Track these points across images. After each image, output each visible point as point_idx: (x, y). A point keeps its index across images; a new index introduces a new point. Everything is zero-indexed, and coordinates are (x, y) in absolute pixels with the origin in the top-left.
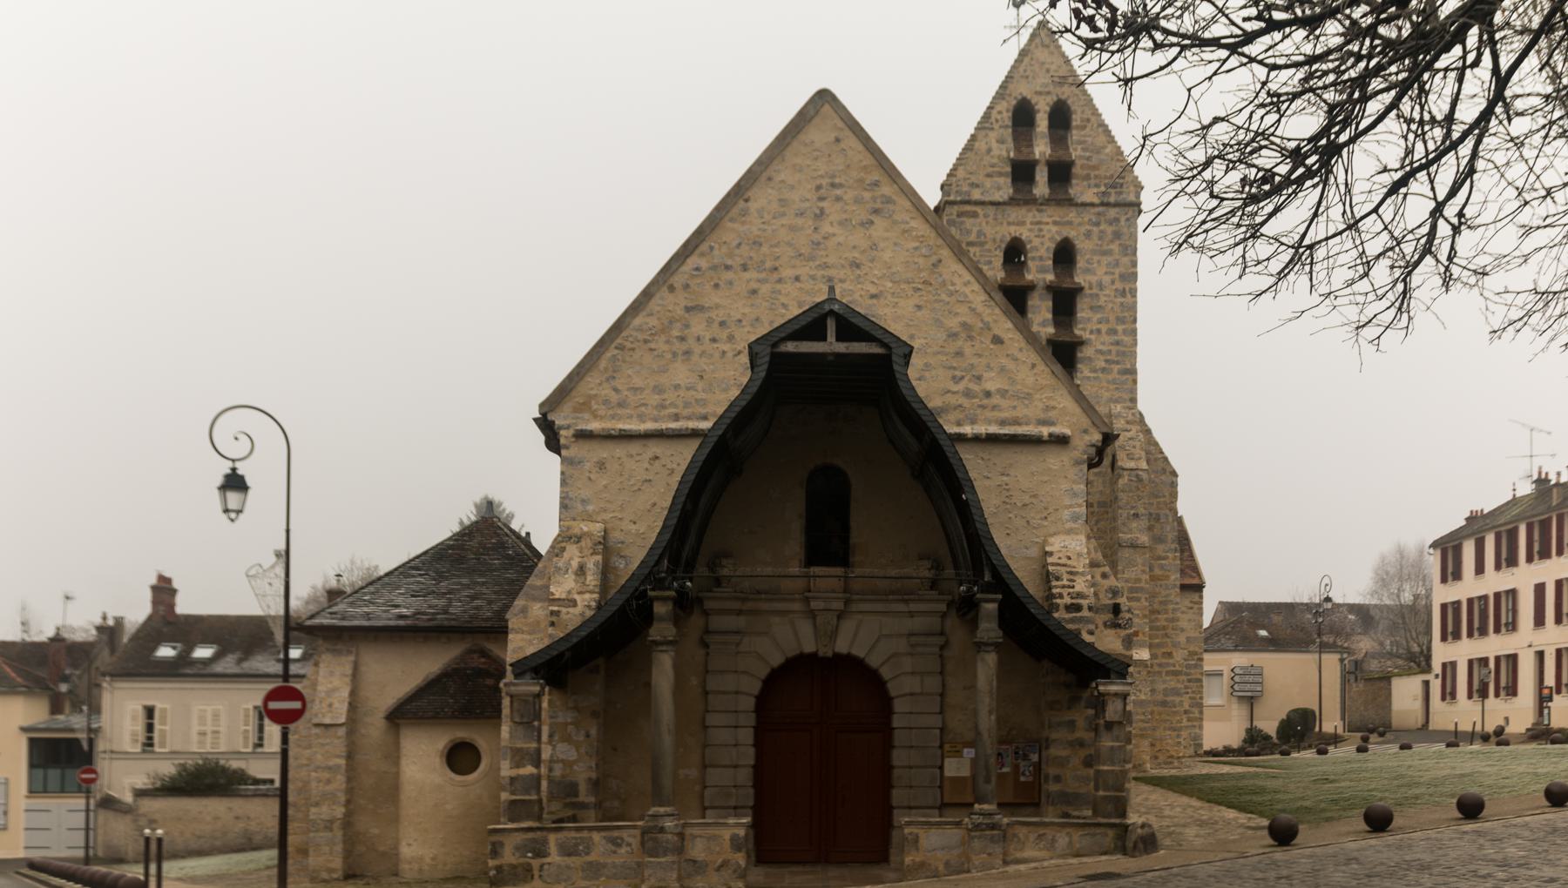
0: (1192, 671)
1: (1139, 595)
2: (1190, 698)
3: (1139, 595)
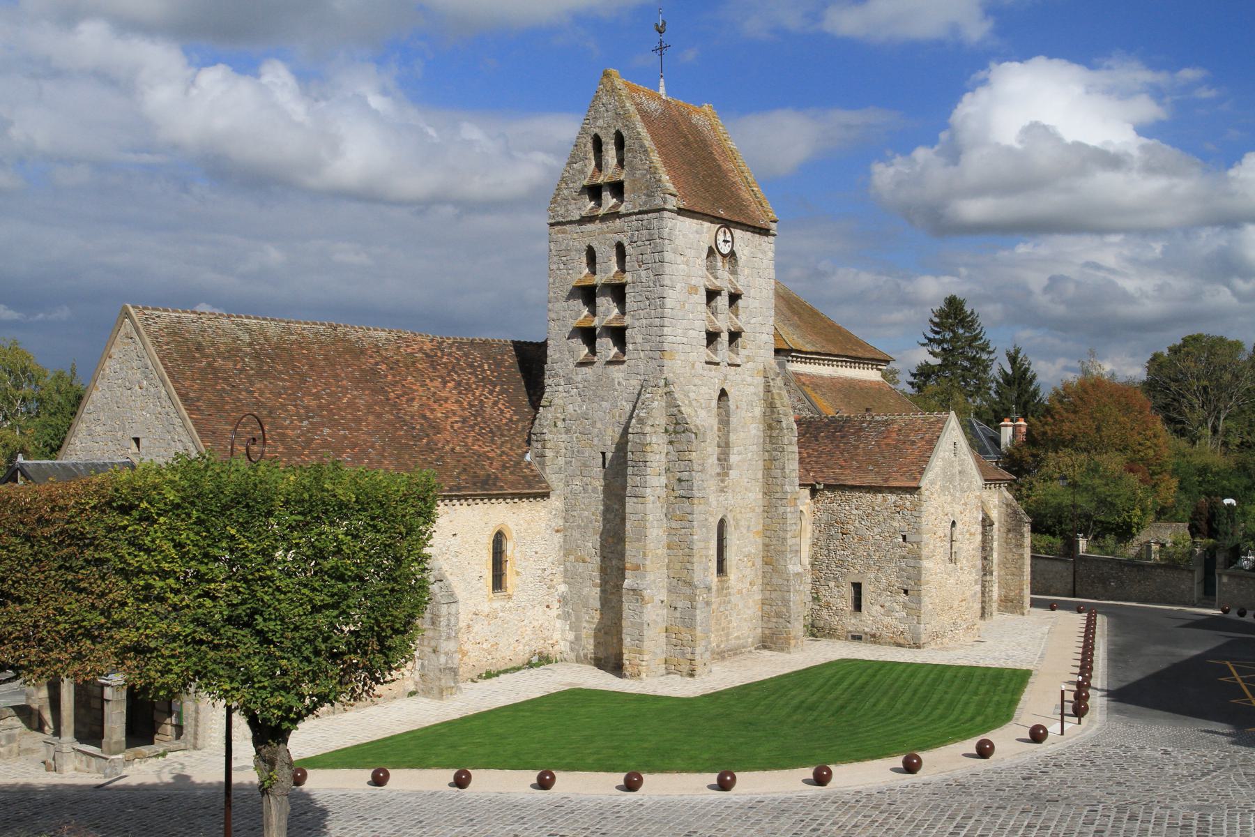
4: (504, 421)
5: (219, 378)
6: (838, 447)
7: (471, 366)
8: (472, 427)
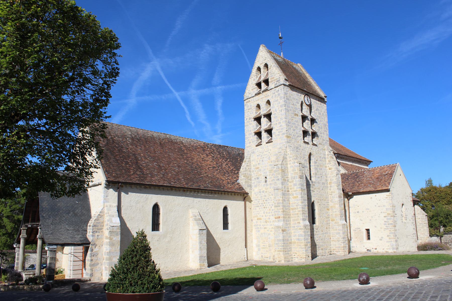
0: (389, 221)
1: (280, 205)
2: (389, 231)
3: (280, 205)
4: (230, 170)
6: (356, 180)
7: (219, 152)
8: (217, 170)
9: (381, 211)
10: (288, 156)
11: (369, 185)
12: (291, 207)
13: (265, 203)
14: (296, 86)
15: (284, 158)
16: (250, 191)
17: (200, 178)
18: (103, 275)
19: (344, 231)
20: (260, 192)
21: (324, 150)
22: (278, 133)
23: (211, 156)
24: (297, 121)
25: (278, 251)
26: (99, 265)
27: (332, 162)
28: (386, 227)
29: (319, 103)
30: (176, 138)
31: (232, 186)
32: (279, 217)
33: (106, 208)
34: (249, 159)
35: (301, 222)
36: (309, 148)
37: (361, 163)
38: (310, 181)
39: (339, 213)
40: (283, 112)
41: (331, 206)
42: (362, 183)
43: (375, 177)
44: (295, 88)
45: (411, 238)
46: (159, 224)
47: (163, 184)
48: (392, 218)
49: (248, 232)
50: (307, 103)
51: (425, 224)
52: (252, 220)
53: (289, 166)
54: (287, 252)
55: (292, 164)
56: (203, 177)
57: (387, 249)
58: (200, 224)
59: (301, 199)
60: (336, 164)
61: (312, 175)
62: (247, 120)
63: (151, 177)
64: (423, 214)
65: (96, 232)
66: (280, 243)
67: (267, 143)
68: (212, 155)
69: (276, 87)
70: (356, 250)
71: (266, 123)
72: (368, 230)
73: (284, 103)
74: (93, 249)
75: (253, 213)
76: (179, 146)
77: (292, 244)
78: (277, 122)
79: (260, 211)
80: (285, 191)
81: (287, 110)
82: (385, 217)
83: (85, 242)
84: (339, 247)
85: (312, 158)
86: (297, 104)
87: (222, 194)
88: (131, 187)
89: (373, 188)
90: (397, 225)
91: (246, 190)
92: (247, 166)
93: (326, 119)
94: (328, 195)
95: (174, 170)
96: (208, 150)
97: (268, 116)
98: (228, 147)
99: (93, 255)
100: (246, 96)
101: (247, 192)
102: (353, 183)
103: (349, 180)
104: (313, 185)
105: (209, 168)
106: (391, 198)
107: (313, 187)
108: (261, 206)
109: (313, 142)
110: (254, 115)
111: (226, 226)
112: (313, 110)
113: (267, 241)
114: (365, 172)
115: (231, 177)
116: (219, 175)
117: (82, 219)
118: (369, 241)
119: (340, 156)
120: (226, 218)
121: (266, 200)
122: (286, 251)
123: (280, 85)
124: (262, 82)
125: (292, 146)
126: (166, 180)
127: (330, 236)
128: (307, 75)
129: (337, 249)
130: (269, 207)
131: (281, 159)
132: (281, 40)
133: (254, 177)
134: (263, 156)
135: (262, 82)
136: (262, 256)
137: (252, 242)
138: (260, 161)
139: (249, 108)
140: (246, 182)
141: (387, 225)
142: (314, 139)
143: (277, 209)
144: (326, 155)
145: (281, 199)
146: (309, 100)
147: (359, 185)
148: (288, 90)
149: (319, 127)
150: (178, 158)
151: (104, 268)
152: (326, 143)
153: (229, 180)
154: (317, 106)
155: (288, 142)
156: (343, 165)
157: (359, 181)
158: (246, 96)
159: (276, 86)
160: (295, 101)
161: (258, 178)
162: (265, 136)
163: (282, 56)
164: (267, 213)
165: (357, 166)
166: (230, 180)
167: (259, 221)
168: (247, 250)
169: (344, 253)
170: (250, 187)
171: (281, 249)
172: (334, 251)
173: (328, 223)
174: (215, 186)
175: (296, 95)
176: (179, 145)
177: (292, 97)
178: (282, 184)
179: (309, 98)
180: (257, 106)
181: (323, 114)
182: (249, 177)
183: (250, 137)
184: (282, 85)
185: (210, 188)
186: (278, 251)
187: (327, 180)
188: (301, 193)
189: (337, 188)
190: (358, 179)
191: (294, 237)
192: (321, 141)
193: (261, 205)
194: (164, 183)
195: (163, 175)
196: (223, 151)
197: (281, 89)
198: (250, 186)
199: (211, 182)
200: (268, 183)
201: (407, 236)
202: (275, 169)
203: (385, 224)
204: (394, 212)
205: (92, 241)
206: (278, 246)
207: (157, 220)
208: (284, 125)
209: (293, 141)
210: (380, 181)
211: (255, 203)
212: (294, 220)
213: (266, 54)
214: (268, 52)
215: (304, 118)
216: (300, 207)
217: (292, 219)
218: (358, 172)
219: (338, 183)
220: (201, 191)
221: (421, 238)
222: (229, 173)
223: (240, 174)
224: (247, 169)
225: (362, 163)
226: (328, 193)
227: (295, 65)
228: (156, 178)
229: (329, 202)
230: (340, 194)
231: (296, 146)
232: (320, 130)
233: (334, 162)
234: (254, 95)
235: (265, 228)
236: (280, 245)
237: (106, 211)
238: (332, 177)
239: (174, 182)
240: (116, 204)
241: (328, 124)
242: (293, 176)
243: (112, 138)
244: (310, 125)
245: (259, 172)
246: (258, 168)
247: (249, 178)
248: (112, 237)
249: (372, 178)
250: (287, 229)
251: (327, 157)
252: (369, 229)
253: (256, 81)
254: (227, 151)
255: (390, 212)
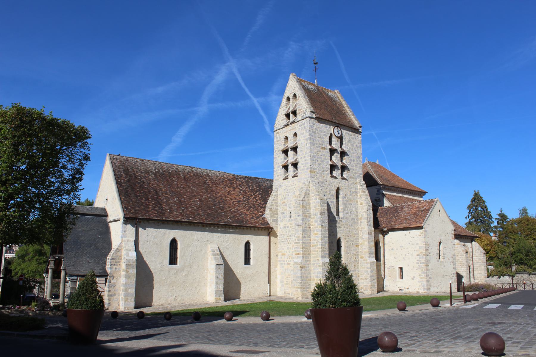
0: (422, 260)
4: (257, 203)
5: (137, 178)
6: (394, 215)
7: (248, 185)
8: (243, 204)
9: (415, 249)
10: (311, 191)
11: (405, 221)
12: (312, 244)
13: (289, 239)
14: (324, 118)
15: (307, 194)
16: (276, 225)
17: (222, 212)
18: (120, 305)
19: (372, 269)
20: (285, 227)
21: (356, 183)
22: (303, 168)
23: (239, 189)
24: (324, 155)
25: (297, 288)
26: (117, 295)
27: (364, 197)
28: (418, 266)
29: (352, 133)
30: (202, 171)
31: (256, 221)
32: (299, 254)
33: (123, 243)
34: (277, 192)
35: (320, 259)
36: (337, 183)
37: (412, 194)
38: (336, 217)
39: (368, 250)
40: (308, 146)
41: (361, 243)
42: (399, 219)
43: (412, 212)
44: (323, 120)
45: (450, 278)
46: (177, 258)
47: (182, 219)
48: (425, 256)
49: (272, 267)
50: (337, 135)
51: (482, 262)
52: (277, 256)
53: (311, 202)
54: (305, 289)
55: (314, 200)
56: (225, 212)
57: (418, 289)
58: (218, 259)
59: (320, 235)
60: (368, 199)
61: (340, 210)
62: (276, 152)
63: (170, 213)
64: (481, 252)
65: (114, 265)
66: (298, 279)
67: (293, 177)
68: (240, 188)
69: (302, 119)
70: (389, 289)
71: (292, 156)
72: (401, 269)
73: (309, 137)
74: (110, 281)
75: (278, 249)
76: (205, 179)
77: (312, 281)
78: (303, 156)
79: (285, 246)
80: (306, 227)
81: (312, 144)
82: (418, 255)
83: (103, 274)
84: (367, 286)
85: (341, 193)
86: (325, 137)
87: (244, 228)
88: (149, 223)
89: (408, 225)
90: (430, 264)
91: (270, 225)
92: (274, 200)
93: (360, 151)
94: (359, 232)
95: (195, 206)
96: (236, 183)
97: (295, 149)
98: (260, 179)
99: (110, 286)
100: (276, 127)
101: (271, 227)
102: (391, 218)
103: (388, 214)
104: (339, 221)
105: (234, 202)
106: (424, 236)
107: (339, 223)
108: (285, 241)
109: (344, 176)
110: (282, 147)
111: (247, 260)
112: (344, 142)
113: (289, 277)
114: (404, 207)
115: (257, 211)
116: (244, 209)
117: (103, 253)
118: (402, 280)
119: (386, 187)
120: (248, 253)
121: (290, 236)
122: (304, 288)
123: (306, 118)
124: (291, 113)
125: (316, 181)
126: (185, 216)
127: (359, 274)
128: (344, 103)
129: (365, 287)
130: (292, 243)
131: (303, 195)
132: (315, 65)
133: (280, 212)
134: (289, 191)
135: (291, 113)
136: (285, 292)
137: (276, 277)
138: (286, 196)
139: (278, 139)
140: (271, 217)
141: (419, 264)
142: (344, 173)
143: (297, 246)
144: (358, 189)
145: (301, 235)
146: (340, 131)
147: (396, 220)
148: (315, 122)
149: (351, 160)
150: (201, 192)
151: (121, 298)
152: (358, 176)
153: (254, 215)
154: (350, 137)
155: (311, 177)
156: (389, 196)
157: (397, 216)
158: (276, 127)
159: (303, 118)
160: (323, 134)
161: (284, 213)
162: (291, 170)
163: (315, 84)
164: (290, 249)
165: (407, 198)
166: (255, 214)
167: (283, 256)
168: (270, 286)
169: (371, 292)
170: (275, 222)
171: (299, 285)
172: (361, 290)
173: (356, 261)
174: (237, 221)
175: (324, 128)
176: (205, 178)
177: (319, 129)
178: (303, 220)
179: (339, 129)
180: (285, 138)
181: (356, 145)
182: (275, 211)
183: (278, 170)
184: (307, 117)
185: (231, 223)
186: (297, 288)
187: (357, 216)
188: (321, 230)
189: (367, 224)
190: (397, 214)
191: (314, 274)
192: (352, 175)
193: (285, 240)
194: (183, 219)
195: (183, 210)
196: (253, 183)
197: (307, 122)
198: (276, 221)
199: (233, 217)
200: (292, 218)
201: (443, 276)
202: (297, 205)
203: (417, 263)
204: (427, 250)
205: (110, 273)
206: (297, 283)
207: (175, 254)
208: (308, 159)
209: (318, 175)
210: (416, 217)
211: (280, 239)
212: (314, 257)
213: (295, 84)
214: (297, 81)
215: (332, 151)
216: (319, 244)
217: (312, 256)
218: (398, 207)
219: (368, 219)
220: (220, 226)
221: (477, 277)
222: (255, 207)
223: (266, 208)
224: (273, 203)
225: (414, 194)
226: (358, 229)
227: (331, 92)
228: (175, 213)
229: (359, 238)
230: (370, 230)
231: (321, 181)
232: (352, 163)
233: (365, 197)
234: (283, 126)
235: (288, 264)
236: (298, 282)
237: (124, 246)
238: (363, 212)
239: (193, 218)
240: (134, 239)
241: (362, 156)
242: (315, 212)
243: (134, 174)
244: (339, 159)
245: (285, 207)
246: (284, 202)
247: (275, 212)
248: (128, 270)
249: (409, 214)
250: (307, 266)
251: (358, 191)
252: (402, 268)
253: (284, 113)
254: (258, 183)
255: (423, 251)
